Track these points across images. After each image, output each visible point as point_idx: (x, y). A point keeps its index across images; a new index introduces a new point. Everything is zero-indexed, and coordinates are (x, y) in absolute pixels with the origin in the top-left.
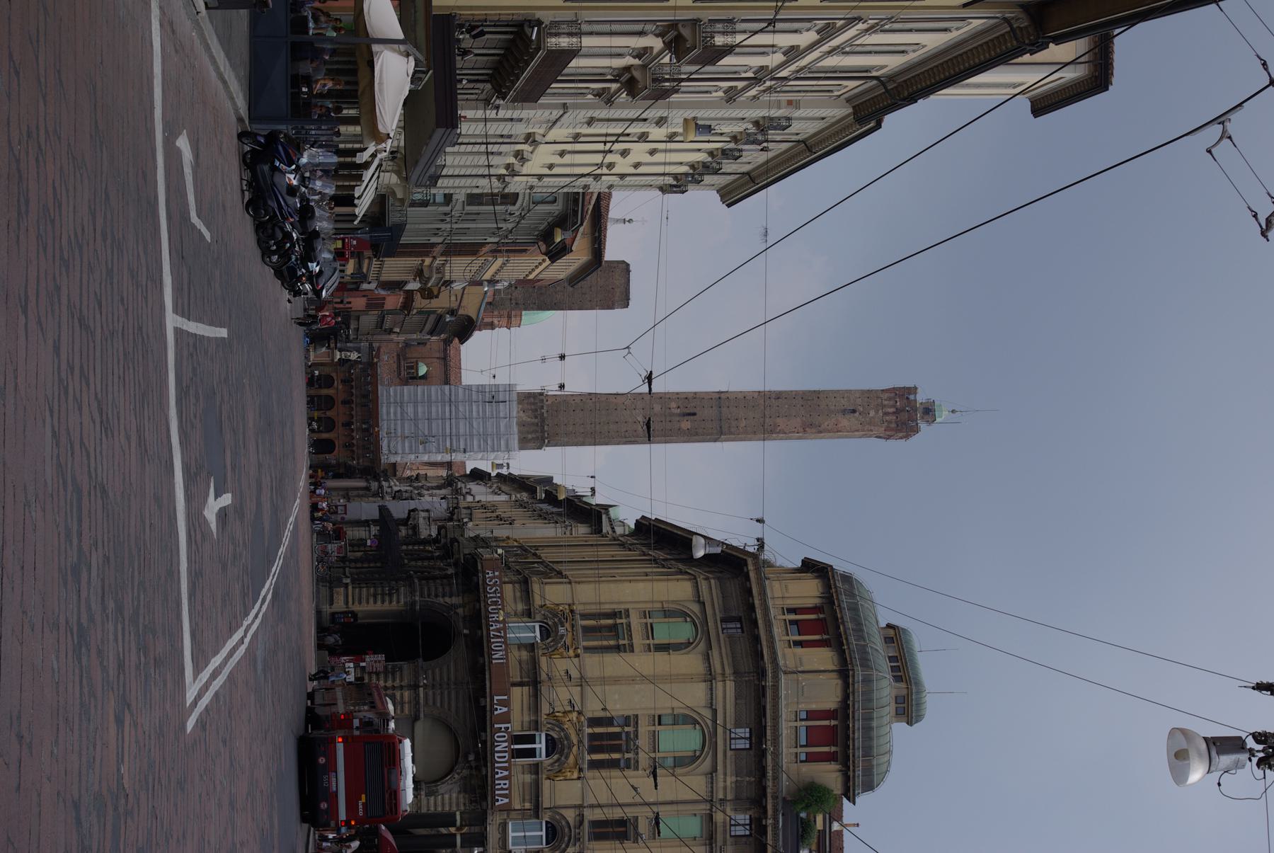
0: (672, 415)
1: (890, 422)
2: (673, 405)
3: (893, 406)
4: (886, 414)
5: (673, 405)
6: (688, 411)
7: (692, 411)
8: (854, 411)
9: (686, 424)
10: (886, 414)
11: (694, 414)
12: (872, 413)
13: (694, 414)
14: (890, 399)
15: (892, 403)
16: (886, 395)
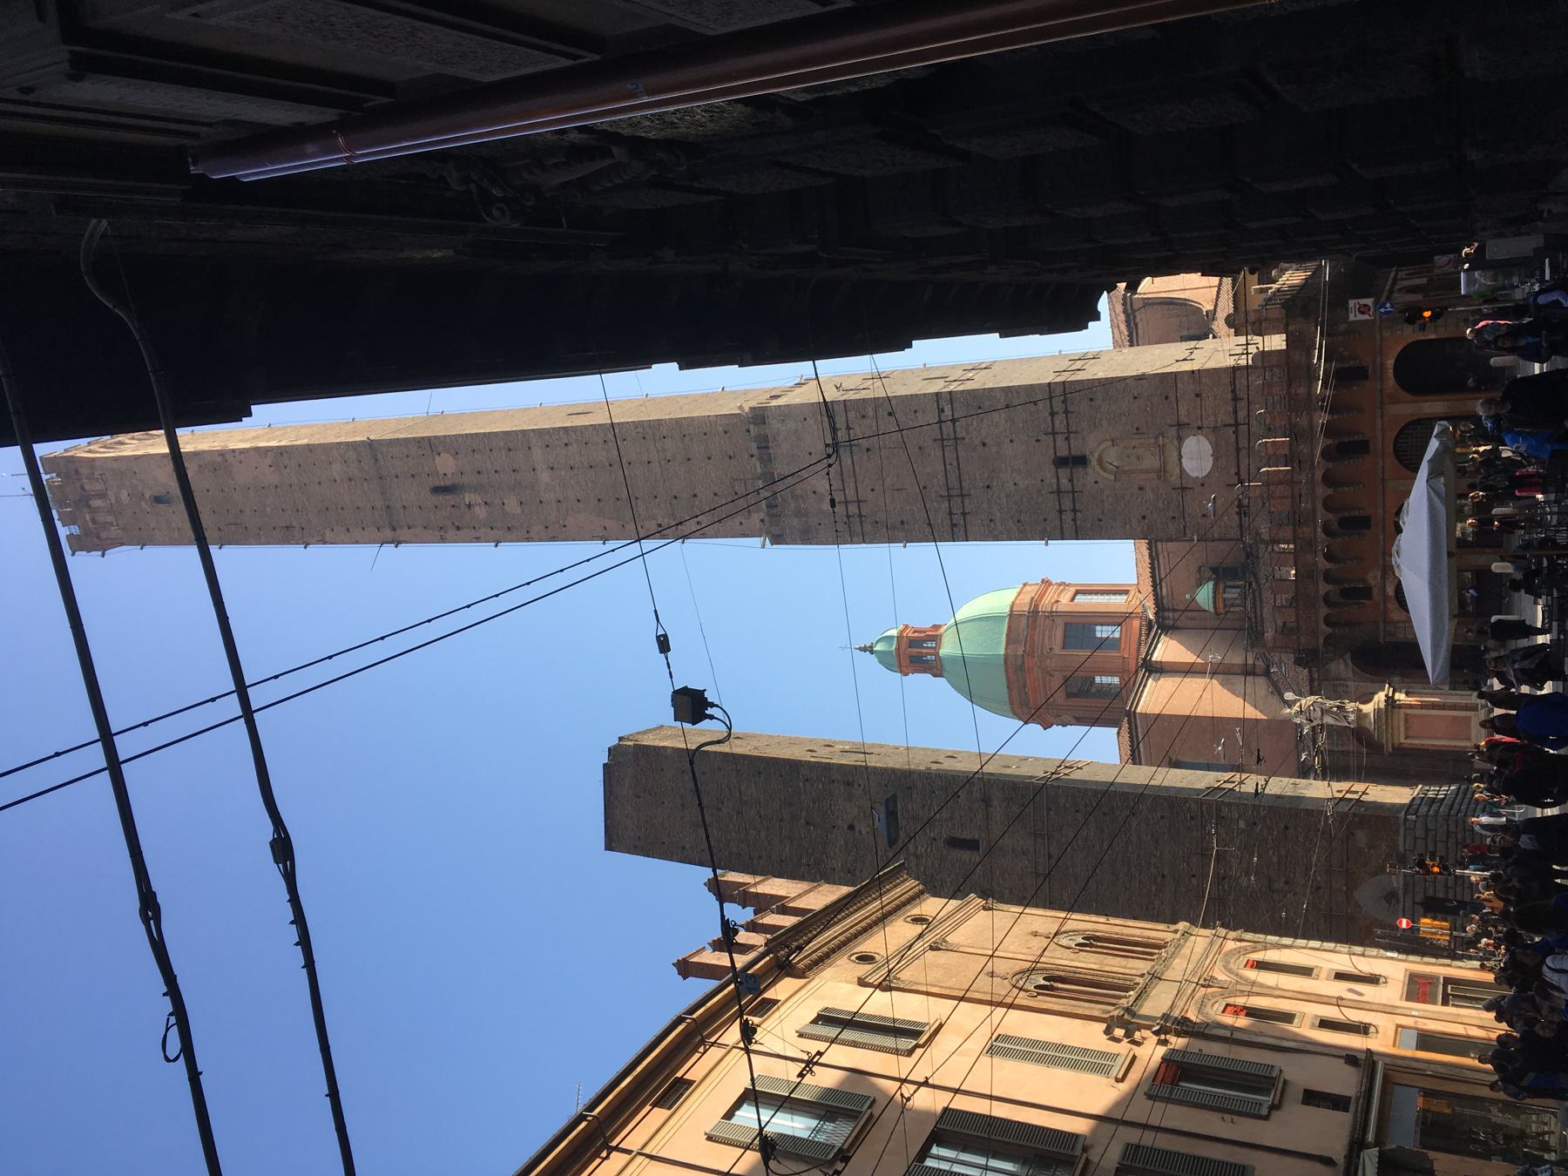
1: (90, 477)
2: (481, 512)
3: (93, 511)
4: (102, 495)
5: (481, 512)
6: (449, 499)
7: (442, 499)
8: (158, 500)
9: (446, 465)
10: (102, 495)
11: (437, 490)
12: (124, 494)
13: (437, 490)
14: (106, 525)
15: (101, 518)
16: (114, 532)
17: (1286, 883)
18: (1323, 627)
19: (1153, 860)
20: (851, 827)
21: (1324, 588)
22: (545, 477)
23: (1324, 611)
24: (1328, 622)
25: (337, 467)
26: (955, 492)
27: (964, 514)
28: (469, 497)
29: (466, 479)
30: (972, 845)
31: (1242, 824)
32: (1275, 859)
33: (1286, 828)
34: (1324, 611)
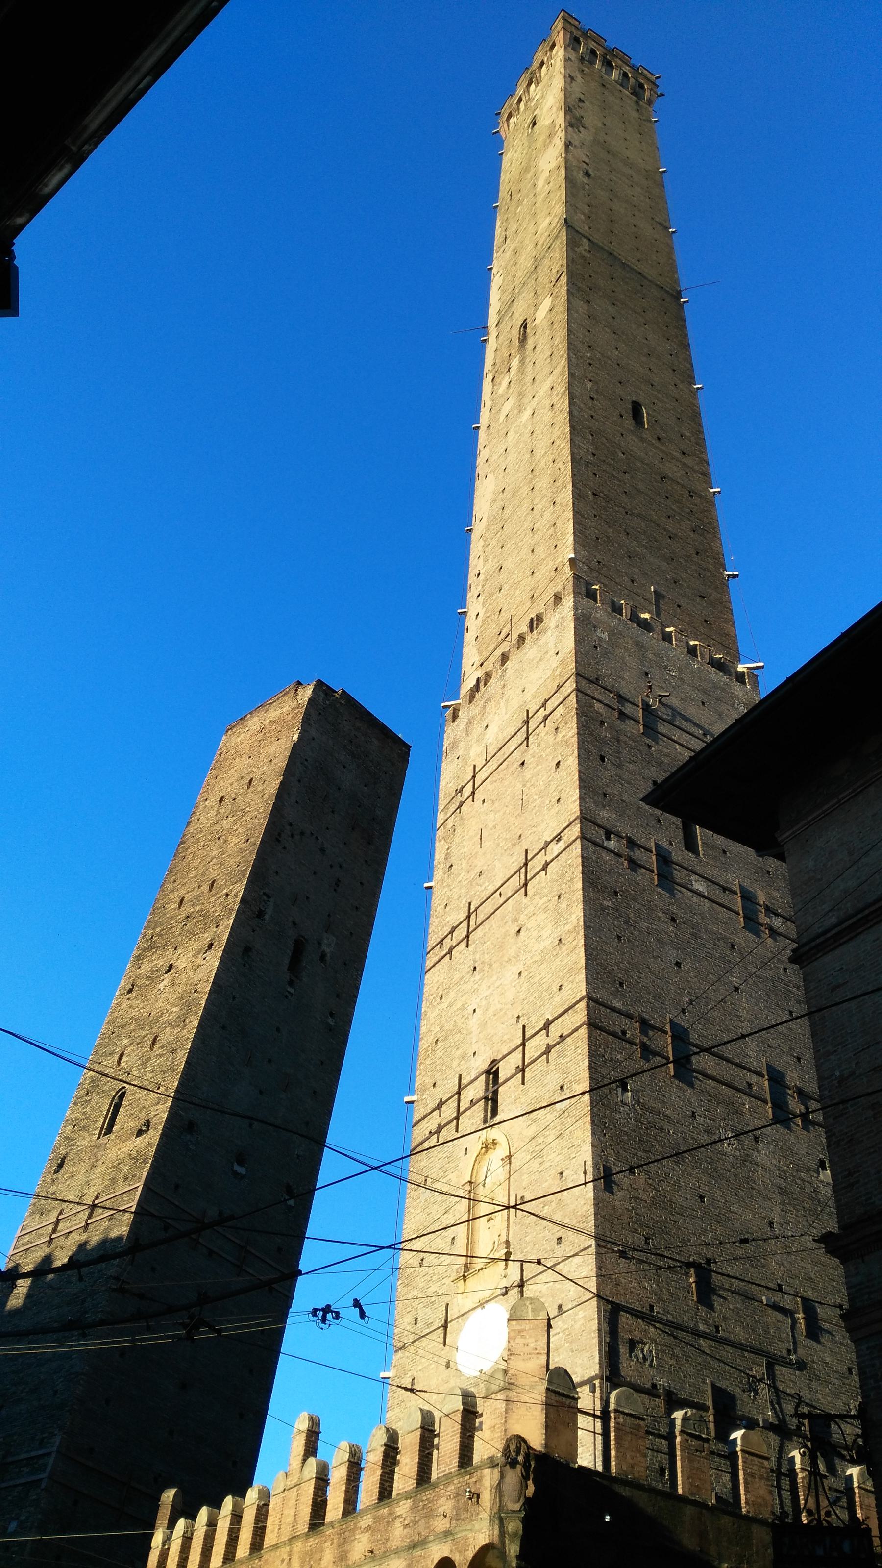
0: (522, 362)
2: (505, 384)
26: (472, 923)
27: (450, 952)
29: (530, 342)
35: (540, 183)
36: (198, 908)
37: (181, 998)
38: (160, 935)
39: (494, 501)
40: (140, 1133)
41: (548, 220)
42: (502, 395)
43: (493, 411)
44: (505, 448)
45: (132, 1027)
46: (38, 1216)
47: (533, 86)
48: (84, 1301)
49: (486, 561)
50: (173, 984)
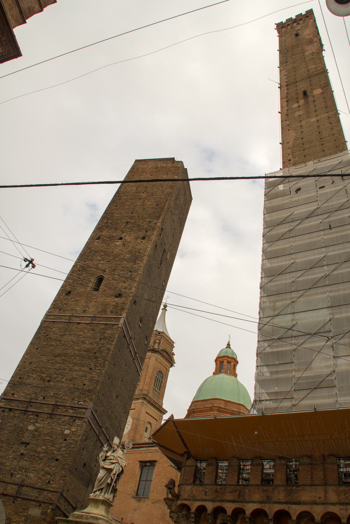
0: (307, 103)
5: (296, 105)
17: (22, 454)
18: (197, 504)
19: (60, 377)
20: (121, 239)
21: (230, 508)
22: (313, 120)
23: (210, 506)
24: (202, 509)
25: (314, 66)
28: (302, 102)
29: (311, 99)
30: (96, 289)
31: (67, 432)
32: (39, 449)
33: (57, 460)
34: (210, 506)
35: (307, 53)
36: (133, 221)
37: (131, 252)
38: (111, 224)
39: (295, 140)
40: (116, 297)
41: (314, 66)
42: (294, 108)
43: (289, 111)
44: (300, 125)
45: (102, 253)
46: (58, 310)
47: (295, 24)
48: (95, 353)
49: (294, 157)
50: (124, 245)
